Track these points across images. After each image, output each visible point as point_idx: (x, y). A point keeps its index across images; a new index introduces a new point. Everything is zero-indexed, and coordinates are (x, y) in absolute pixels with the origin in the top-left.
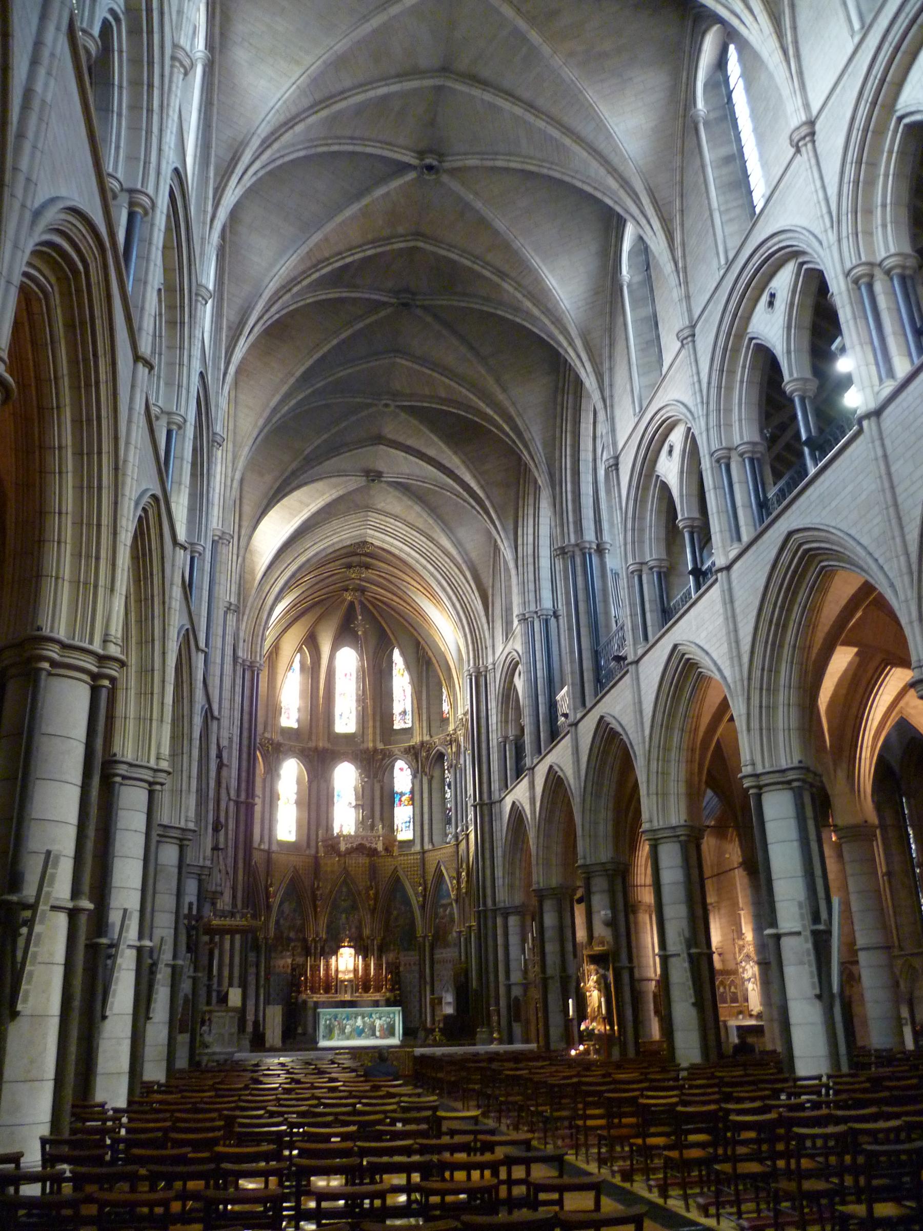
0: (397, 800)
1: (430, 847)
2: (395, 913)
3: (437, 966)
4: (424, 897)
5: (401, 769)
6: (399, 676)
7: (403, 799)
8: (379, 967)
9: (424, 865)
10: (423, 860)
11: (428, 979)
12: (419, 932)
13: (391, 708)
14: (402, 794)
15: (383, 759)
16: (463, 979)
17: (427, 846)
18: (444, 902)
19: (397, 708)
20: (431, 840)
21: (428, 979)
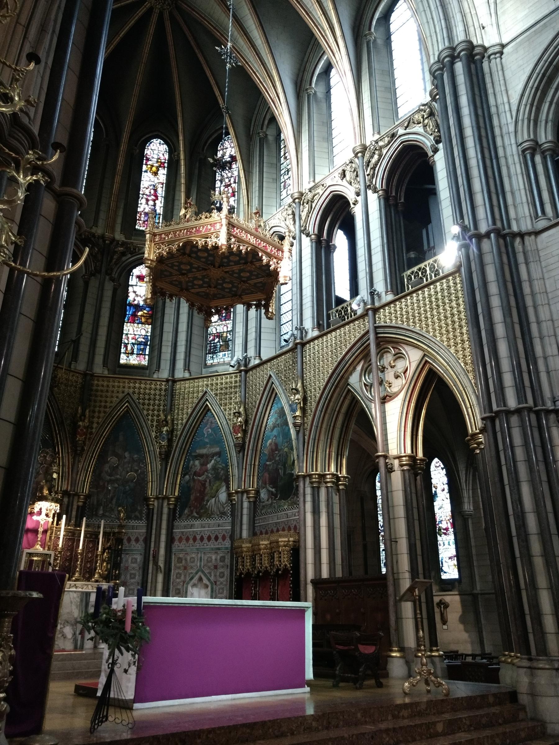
0: (130, 312)
1: (187, 375)
2: (113, 460)
3: (176, 546)
4: (170, 441)
5: (141, 278)
6: (149, 174)
7: (140, 313)
8: (92, 538)
9: (172, 396)
10: (171, 394)
11: (161, 564)
12: (151, 491)
13: (136, 205)
14: (138, 307)
15: (123, 254)
16: (286, 561)
17: (180, 373)
18: (204, 451)
19: (143, 206)
20: (187, 367)
21: (161, 564)
